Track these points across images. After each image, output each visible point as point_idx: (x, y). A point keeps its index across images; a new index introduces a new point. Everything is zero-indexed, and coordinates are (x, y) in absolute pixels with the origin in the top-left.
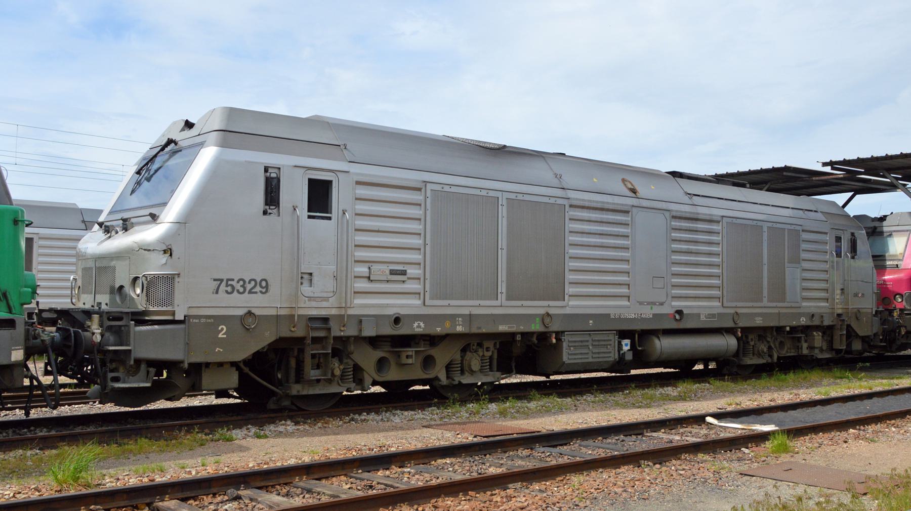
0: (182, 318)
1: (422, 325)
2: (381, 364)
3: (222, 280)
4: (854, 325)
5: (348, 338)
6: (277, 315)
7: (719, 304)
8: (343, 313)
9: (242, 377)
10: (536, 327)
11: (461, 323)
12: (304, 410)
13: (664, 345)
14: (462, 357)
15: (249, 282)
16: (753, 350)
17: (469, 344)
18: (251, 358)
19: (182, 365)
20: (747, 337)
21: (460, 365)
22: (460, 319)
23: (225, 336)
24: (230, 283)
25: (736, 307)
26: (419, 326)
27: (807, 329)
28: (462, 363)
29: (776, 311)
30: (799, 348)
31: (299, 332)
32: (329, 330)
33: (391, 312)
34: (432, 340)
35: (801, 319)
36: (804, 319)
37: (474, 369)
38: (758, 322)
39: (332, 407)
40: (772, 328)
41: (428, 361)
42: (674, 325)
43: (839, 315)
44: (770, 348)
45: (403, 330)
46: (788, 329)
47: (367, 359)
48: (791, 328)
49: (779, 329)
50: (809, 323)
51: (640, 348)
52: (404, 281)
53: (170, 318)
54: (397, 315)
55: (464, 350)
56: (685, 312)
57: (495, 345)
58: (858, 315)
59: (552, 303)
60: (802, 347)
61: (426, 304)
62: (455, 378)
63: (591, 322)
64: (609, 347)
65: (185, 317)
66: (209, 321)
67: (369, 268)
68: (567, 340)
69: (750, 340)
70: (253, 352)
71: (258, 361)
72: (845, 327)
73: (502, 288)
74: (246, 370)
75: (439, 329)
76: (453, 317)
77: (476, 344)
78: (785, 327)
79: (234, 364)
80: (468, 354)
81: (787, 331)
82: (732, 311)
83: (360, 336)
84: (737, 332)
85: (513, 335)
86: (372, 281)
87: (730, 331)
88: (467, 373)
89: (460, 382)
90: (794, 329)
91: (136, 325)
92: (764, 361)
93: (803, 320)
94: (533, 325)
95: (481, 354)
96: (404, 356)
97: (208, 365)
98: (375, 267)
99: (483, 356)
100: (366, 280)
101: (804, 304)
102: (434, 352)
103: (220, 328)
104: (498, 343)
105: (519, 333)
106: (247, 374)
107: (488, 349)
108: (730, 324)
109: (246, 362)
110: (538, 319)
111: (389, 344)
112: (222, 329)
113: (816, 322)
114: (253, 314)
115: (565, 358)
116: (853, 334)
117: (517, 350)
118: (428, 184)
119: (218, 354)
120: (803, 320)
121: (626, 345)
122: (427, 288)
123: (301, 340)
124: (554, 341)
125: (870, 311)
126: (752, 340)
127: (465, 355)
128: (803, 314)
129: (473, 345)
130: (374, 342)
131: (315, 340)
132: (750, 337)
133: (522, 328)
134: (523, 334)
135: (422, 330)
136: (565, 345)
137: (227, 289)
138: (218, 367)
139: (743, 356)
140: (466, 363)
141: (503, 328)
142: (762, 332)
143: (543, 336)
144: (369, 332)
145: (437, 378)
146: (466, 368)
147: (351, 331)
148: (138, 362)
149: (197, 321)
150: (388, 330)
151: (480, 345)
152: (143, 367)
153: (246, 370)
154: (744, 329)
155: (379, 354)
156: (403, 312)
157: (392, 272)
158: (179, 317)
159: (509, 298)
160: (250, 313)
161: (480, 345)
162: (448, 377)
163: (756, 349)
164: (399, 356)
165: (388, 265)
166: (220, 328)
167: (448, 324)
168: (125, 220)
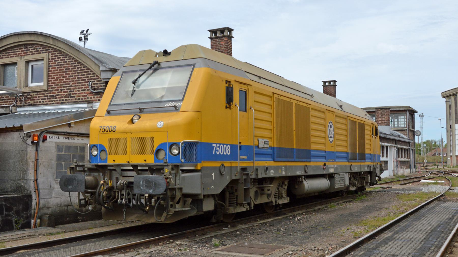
6: (231, 167)
8: (237, 165)
26: (272, 173)
34: (272, 180)
46: (363, 173)
49: (360, 173)
60: (363, 182)
61: (275, 160)
65: (201, 167)
67: (258, 140)
78: (362, 172)
79: (213, 196)
83: (256, 178)
91: (182, 173)
111: (257, 183)
114: (224, 166)
118: (274, 94)
140: (280, 193)
145: (272, 202)
146: (280, 195)
164: (263, 190)
165: (263, 138)
168: (140, 109)
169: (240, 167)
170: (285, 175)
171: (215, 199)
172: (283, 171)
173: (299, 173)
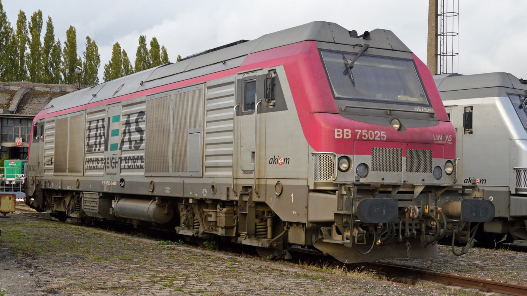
35: (203, 191)
36: (206, 191)
38: (167, 192)
82: (149, 180)
93: (205, 193)
120: (205, 193)
128: (204, 185)
159: (69, 172)
170: (60, 189)
173: (70, 187)
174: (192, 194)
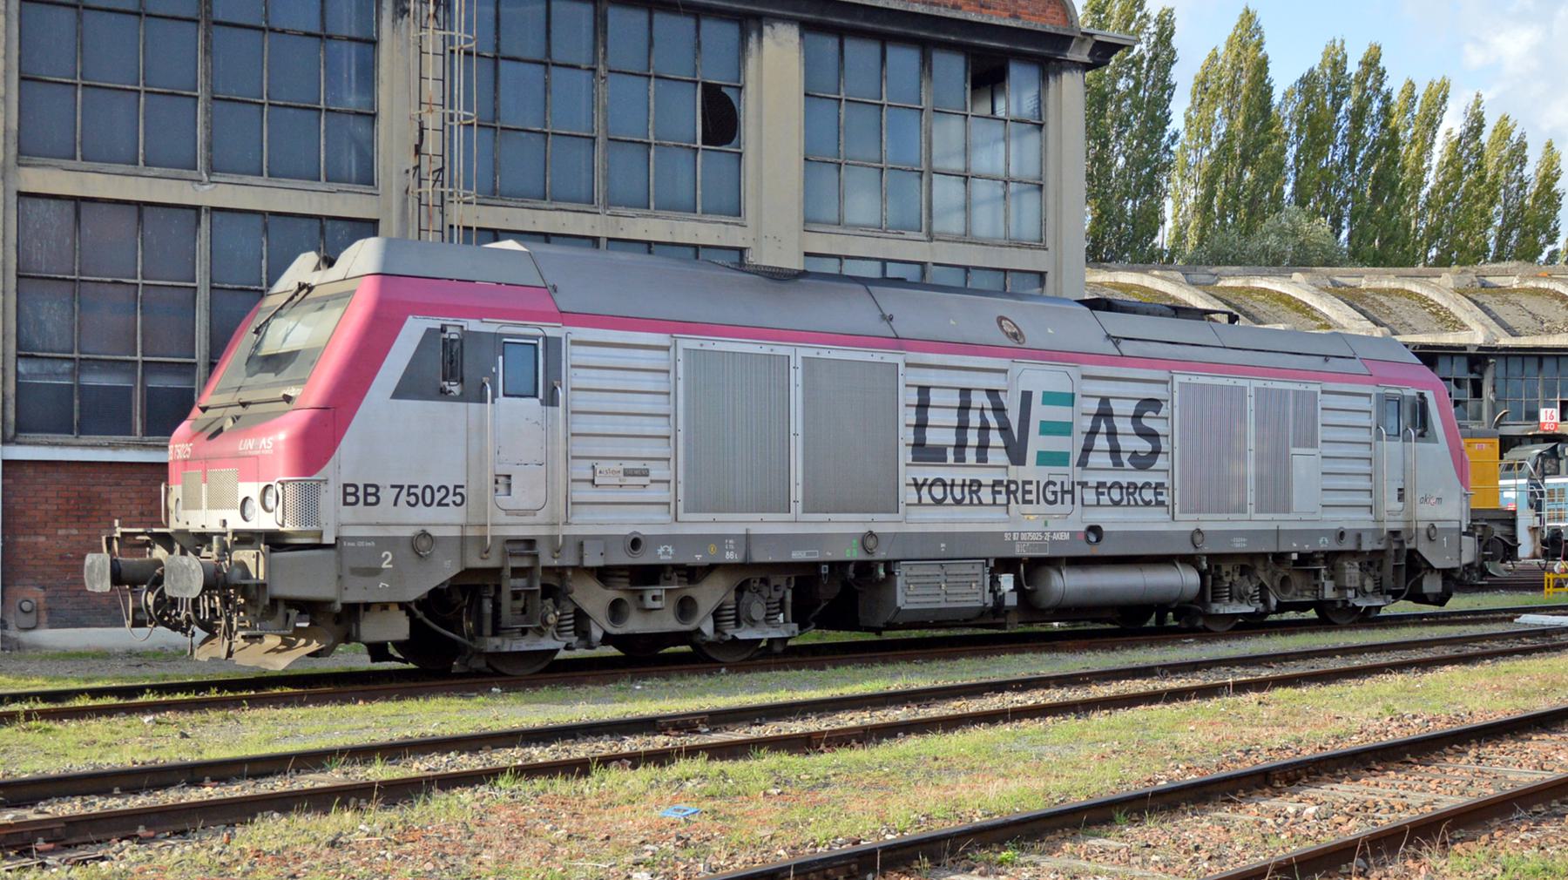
0: (333, 542)
1: (670, 550)
2: (616, 610)
3: (401, 487)
4: (1424, 549)
5: (563, 569)
7: (1169, 517)
9: (415, 625)
10: (853, 553)
11: (732, 547)
12: (505, 675)
13: (1067, 583)
14: (737, 599)
15: (439, 491)
16: (1230, 592)
17: (748, 581)
18: (426, 597)
19: (332, 605)
20: (1218, 568)
21: (733, 612)
22: (731, 541)
23: (391, 566)
24: (412, 490)
25: (1198, 520)
26: (666, 553)
27: (1331, 557)
28: (737, 609)
29: (1273, 527)
30: (1317, 588)
31: (493, 562)
32: (536, 556)
33: (626, 531)
35: (1321, 541)
37: (755, 618)
38: (1238, 545)
39: (541, 672)
40: (1264, 555)
41: (686, 608)
42: (1085, 550)
43: (1395, 533)
44: (1262, 587)
45: (643, 558)
46: (1295, 557)
47: (594, 599)
48: (1300, 555)
49: (1280, 557)
50: (1336, 547)
51: (1029, 588)
52: (645, 486)
53: (316, 541)
54: (635, 536)
55: (740, 590)
56: (1104, 529)
57: (788, 582)
58: (1432, 532)
59: (877, 517)
62: (727, 631)
63: (943, 545)
64: (974, 585)
65: (336, 538)
66: (369, 544)
68: (903, 574)
69: (1224, 574)
70: (430, 589)
71: (437, 601)
72: (1405, 554)
73: (797, 493)
74: (420, 614)
75: (699, 557)
76: (720, 539)
77: (758, 581)
79: (403, 606)
80: (746, 594)
81: (1294, 561)
82: (1191, 527)
84: (1200, 562)
85: (816, 565)
86: (597, 486)
87: (1188, 560)
88: (744, 624)
89: (734, 637)
90: (1305, 558)
92: (1252, 610)
93: (1324, 542)
94: (848, 551)
95: (767, 596)
96: (648, 597)
97: (368, 606)
98: (602, 466)
99: (770, 597)
100: (589, 485)
101: (1330, 515)
102: (692, 591)
103: (383, 555)
104: (793, 579)
105: (825, 563)
106: (420, 620)
107: (776, 588)
108: (1188, 549)
109: (420, 603)
110: (855, 541)
111: (627, 580)
112: (387, 556)
113: (1348, 545)
115: (901, 601)
116: (1424, 566)
117: (828, 591)
119: (380, 590)
120: (1324, 542)
121: (1007, 582)
122: (681, 496)
123: (496, 572)
124: (882, 573)
125: (1456, 525)
126: (1228, 574)
127: (742, 596)
129: (755, 582)
130: (604, 575)
131: (517, 572)
132: (1226, 568)
133: (830, 556)
134: (832, 564)
135: (670, 557)
136: (900, 582)
137: (408, 499)
138: (382, 610)
139: (1213, 601)
140: (743, 609)
141: (798, 556)
142: (1247, 563)
143: (865, 568)
144: (593, 560)
145: (698, 631)
147: (569, 560)
148: (274, 601)
149: (353, 544)
150: (623, 558)
151: (765, 581)
152: (281, 609)
153: (420, 614)
154: (1211, 557)
155: (612, 594)
156: (644, 531)
157: (627, 473)
158: (329, 539)
160: (424, 534)
161: (765, 581)
162: (716, 630)
163: (1235, 589)
164: (642, 598)
166: (383, 555)
167: (712, 549)
169: (493, 537)
171: (410, 613)
172: (730, 551)
174: (1294, 547)
